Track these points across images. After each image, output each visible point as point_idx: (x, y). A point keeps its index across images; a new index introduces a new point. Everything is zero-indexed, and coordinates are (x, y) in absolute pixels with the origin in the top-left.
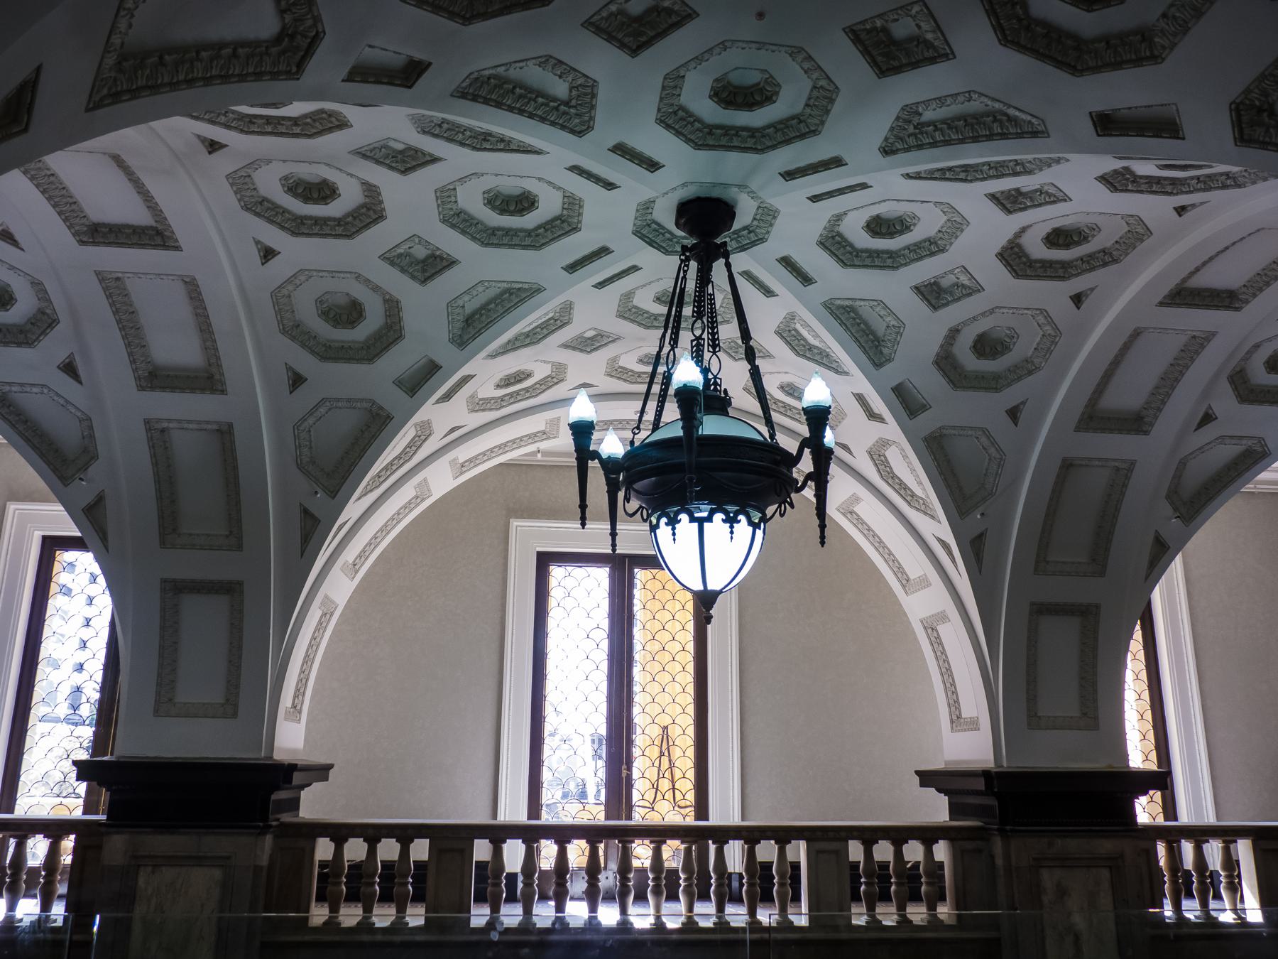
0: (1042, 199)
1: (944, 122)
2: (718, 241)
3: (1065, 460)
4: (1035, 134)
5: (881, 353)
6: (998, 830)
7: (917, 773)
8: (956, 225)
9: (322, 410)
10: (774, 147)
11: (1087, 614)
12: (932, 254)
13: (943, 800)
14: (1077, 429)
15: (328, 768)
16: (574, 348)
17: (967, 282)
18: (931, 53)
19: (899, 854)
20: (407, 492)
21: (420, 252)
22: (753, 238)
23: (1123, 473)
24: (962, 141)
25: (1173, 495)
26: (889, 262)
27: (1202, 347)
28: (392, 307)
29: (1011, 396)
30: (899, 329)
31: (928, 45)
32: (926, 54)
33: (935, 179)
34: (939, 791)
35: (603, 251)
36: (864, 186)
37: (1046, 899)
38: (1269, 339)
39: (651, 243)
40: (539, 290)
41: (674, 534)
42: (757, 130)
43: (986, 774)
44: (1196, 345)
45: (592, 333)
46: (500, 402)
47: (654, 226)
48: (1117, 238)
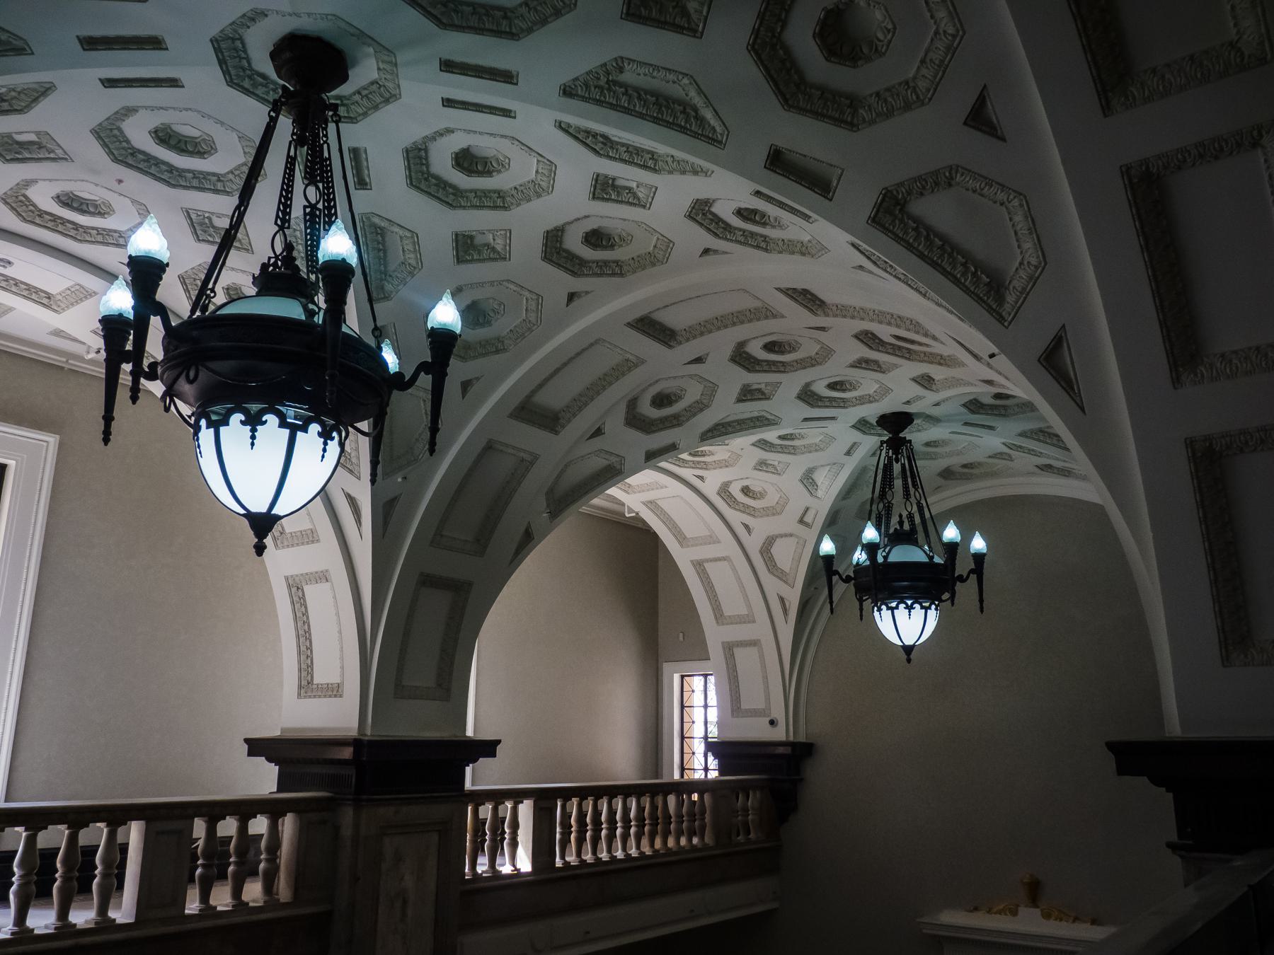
0: (625, 196)
1: (637, 89)
3: (490, 441)
4: (713, 141)
5: (382, 288)
7: (246, 741)
12: (495, 207)
13: (272, 771)
14: (511, 416)
17: (499, 248)
18: (683, 22)
19: (243, 829)
23: (526, 464)
24: (641, 116)
25: (550, 492)
27: (630, 370)
32: (678, 21)
33: (576, 138)
34: (269, 760)
36: (506, 113)
39: (222, 62)
41: (253, 437)
43: (357, 743)
44: (628, 366)
45: (33, 137)
47: (238, 44)
48: (634, 255)
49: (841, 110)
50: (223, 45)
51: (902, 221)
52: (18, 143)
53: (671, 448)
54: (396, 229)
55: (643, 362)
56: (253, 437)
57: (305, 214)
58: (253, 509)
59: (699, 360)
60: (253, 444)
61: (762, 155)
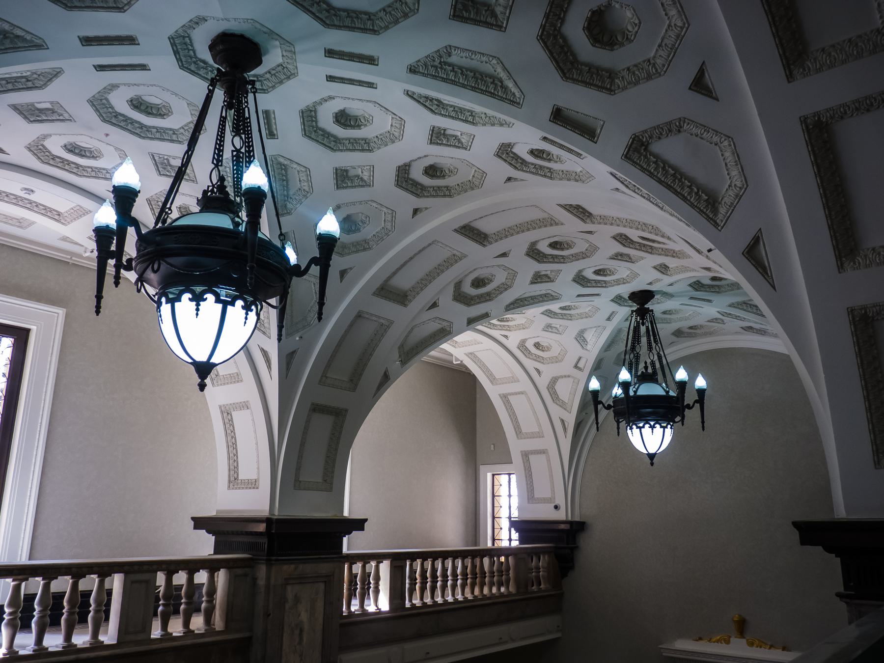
1: (461, 68)
3: (359, 312)
4: (513, 102)
5: (286, 206)
6: (266, 560)
7: (193, 519)
10: (339, 27)
12: (363, 150)
13: (211, 539)
14: (374, 294)
16: (20, 113)
17: (366, 178)
18: (493, 21)
19: (190, 580)
23: (384, 327)
24: (464, 86)
25: (402, 346)
26: (332, 144)
27: (456, 262)
31: (494, 14)
32: (489, 20)
34: (209, 532)
36: (370, 85)
37: (287, 607)
39: (176, 53)
40: (40, 46)
41: (197, 310)
42: (334, 8)
43: (268, 521)
44: (454, 260)
45: (48, 106)
47: (187, 40)
49: (602, 80)
50: (177, 41)
51: (645, 157)
52: (38, 109)
53: (486, 316)
54: (295, 166)
55: (465, 256)
56: (197, 310)
57: (233, 156)
58: (197, 360)
59: (504, 255)
60: (197, 314)
61: (547, 113)
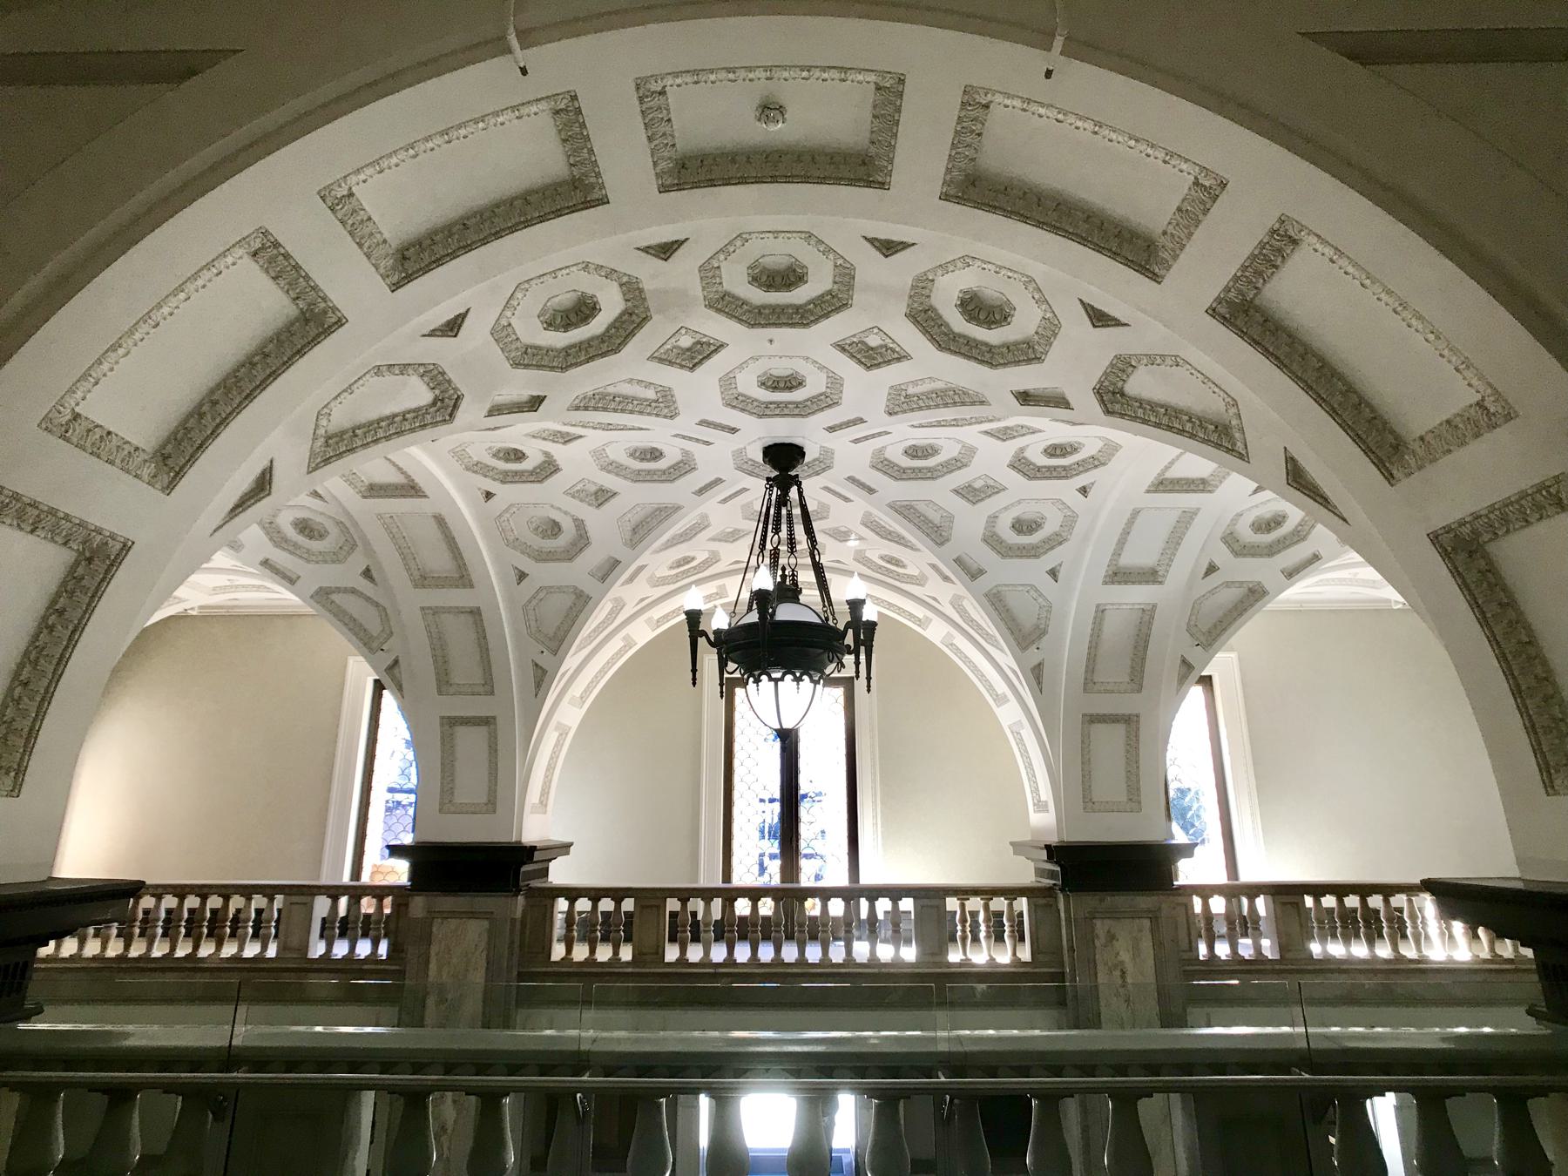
2: (793, 473)
7: (1012, 844)
8: (970, 452)
9: (541, 595)
11: (1129, 721)
15: (569, 845)
20: (616, 644)
21: (593, 489)
22: (824, 464)
25: (1191, 629)
28: (580, 524)
29: (1049, 561)
30: (951, 518)
35: (718, 481)
37: (1097, 943)
38: (1249, 509)
40: (678, 508)
44: (1188, 517)
46: (676, 578)
